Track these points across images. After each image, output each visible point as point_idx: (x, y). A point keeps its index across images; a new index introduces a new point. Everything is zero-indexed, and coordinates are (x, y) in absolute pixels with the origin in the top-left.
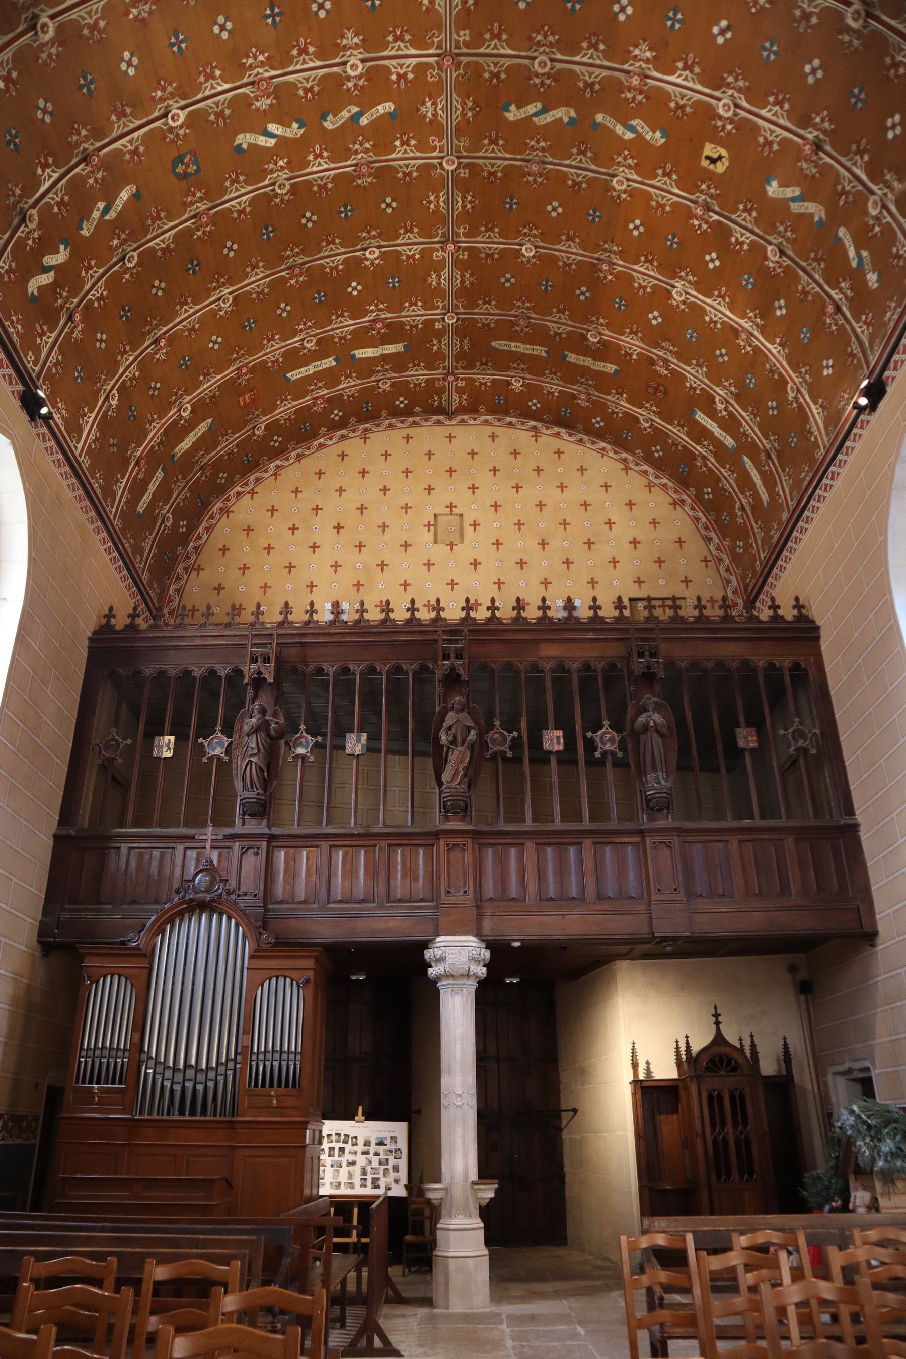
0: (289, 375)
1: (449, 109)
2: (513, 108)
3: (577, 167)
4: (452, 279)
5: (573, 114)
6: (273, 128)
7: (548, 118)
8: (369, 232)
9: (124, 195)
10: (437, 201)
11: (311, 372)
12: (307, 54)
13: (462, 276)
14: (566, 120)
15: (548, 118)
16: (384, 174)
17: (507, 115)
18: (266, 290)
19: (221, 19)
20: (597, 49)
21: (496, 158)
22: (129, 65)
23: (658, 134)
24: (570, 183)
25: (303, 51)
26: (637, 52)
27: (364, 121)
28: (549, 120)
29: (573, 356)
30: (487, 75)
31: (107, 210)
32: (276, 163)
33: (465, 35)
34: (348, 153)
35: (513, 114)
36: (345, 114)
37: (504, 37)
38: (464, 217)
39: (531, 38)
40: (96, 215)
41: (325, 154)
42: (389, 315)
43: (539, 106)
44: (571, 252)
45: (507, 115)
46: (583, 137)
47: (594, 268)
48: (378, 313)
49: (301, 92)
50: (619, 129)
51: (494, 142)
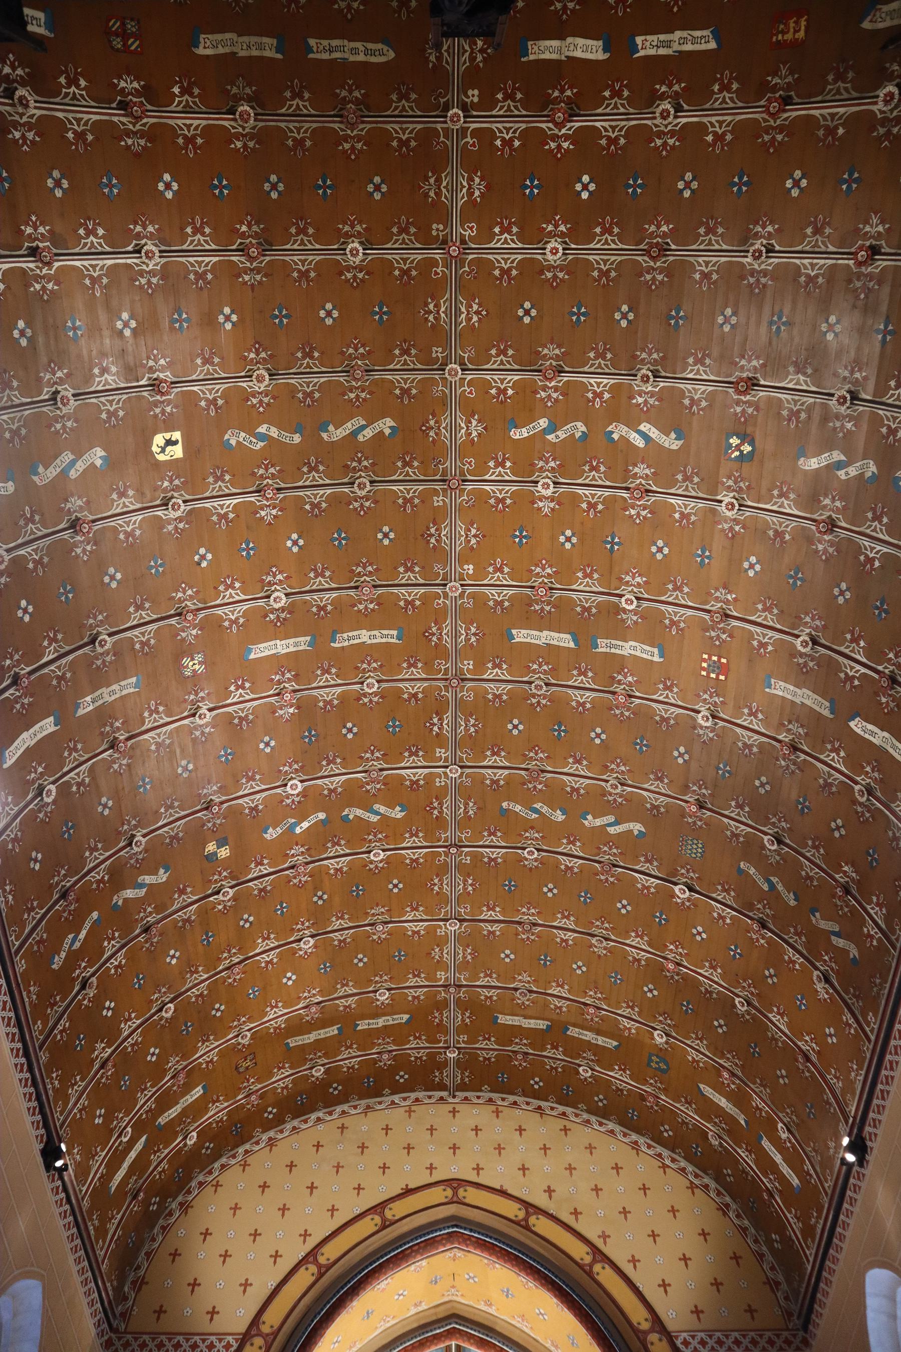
0: (713, 45)
1: (453, 429)
2: (387, 432)
3: (310, 380)
4: (453, 190)
5: (325, 435)
6: (640, 443)
7: (349, 426)
8: (555, 277)
9: (813, 464)
10: (469, 314)
11: (678, 34)
12: (589, 503)
13: (438, 194)
14: (331, 428)
15: (349, 426)
16: (529, 361)
17: (393, 424)
18: (702, 230)
19: (659, 556)
20: (312, 504)
21: (402, 376)
22: (752, 566)
23: (233, 442)
24: (316, 354)
25: (592, 506)
26: (274, 512)
27: (543, 423)
28: (349, 425)
29: (268, 53)
30: (416, 464)
31: (839, 465)
32: (646, 402)
33: (438, 501)
34: (566, 390)
35: (386, 425)
36: (562, 434)
37: (400, 501)
38: (435, 289)
39: (376, 502)
40: (853, 471)
41: (590, 395)
42: (543, 126)
43: (360, 438)
44: (302, 255)
45: (393, 424)
46: (308, 414)
47: (267, 243)
48: (561, 133)
49: (602, 469)
50: (274, 432)
51: (406, 392)
